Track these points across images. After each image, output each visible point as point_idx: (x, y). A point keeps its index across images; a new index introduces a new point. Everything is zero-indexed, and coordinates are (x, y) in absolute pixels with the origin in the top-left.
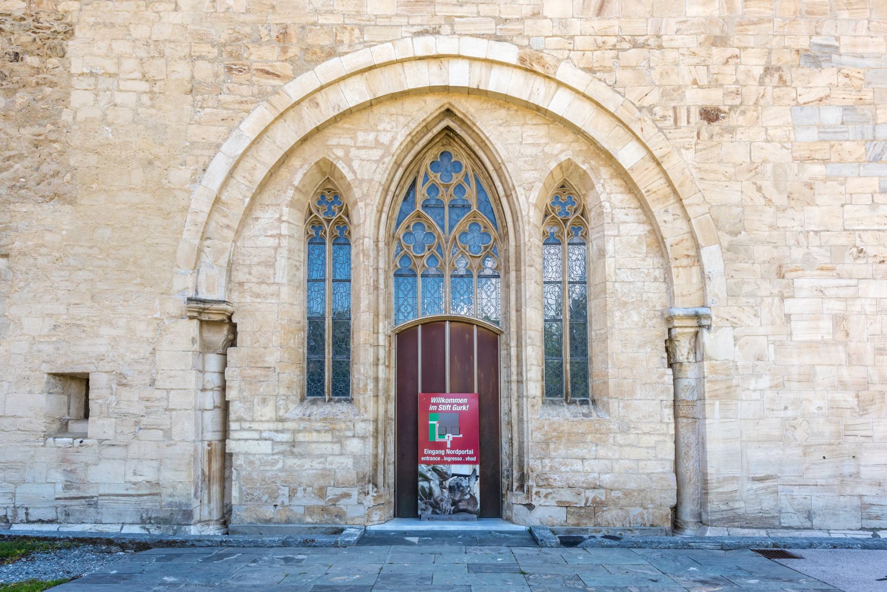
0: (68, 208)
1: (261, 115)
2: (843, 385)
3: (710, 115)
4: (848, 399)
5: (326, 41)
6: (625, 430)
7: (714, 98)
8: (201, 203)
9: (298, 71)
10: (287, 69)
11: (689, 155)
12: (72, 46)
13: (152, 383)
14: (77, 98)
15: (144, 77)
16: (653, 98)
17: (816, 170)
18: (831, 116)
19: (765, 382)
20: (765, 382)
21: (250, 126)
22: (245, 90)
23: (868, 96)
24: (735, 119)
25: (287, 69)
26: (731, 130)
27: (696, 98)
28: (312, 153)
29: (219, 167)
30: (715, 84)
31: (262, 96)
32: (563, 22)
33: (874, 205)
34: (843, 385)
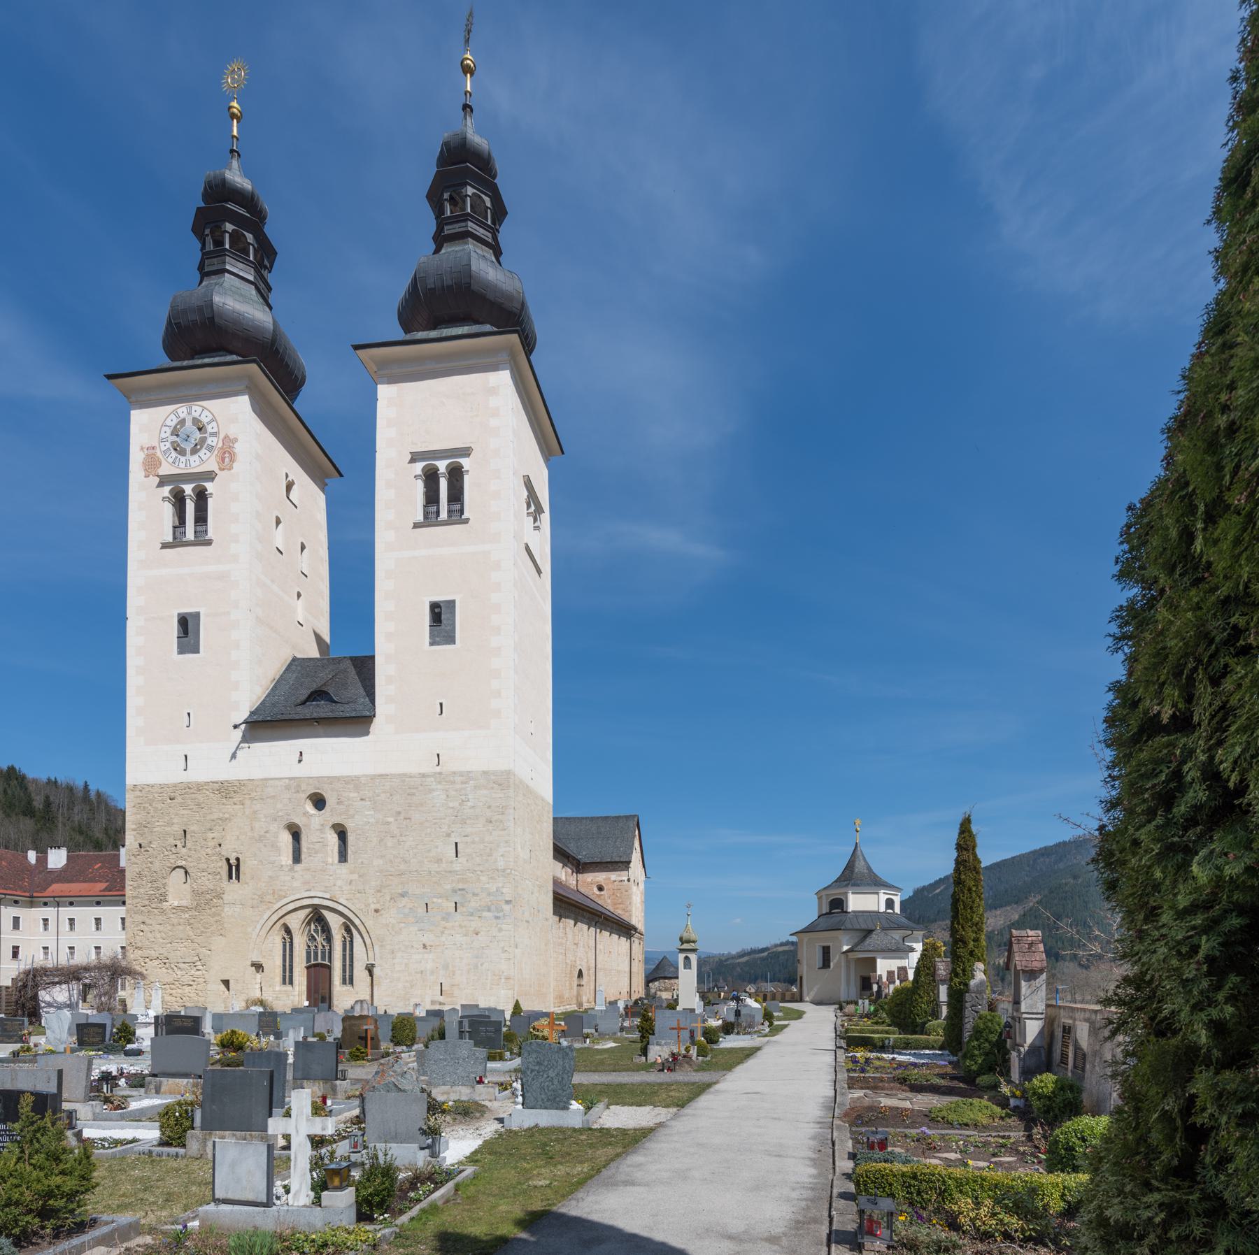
0: (224, 938)
1: (269, 913)
2: (407, 981)
3: (377, 911)
4: (408, 985)
5: (283, 894)
6: (357, 993)
7: (378, 906)
8: (254, 936)
9: (277, 901)
10: (274, 901)
11: (371, 922)
12: (225, 897)
13: (244, 982)
14: (226, 910)
15: (241, 904)
16: (363, 907)
17: (403, 925)
18: (406, 911)
19: (388, 981)
20: (388, 981)
21: (266, 917)
22: (265, 907)
23: (416, 905)
24: (382, 912)
25: (274, 901)
26: (381, 915)
27: (373, 907)
28: (281, 922)
29: (259, 927)
30: (378, 903)
31: (268, 909)
32: (340, 887)
33: (416, 934)
34: (407, 981)
